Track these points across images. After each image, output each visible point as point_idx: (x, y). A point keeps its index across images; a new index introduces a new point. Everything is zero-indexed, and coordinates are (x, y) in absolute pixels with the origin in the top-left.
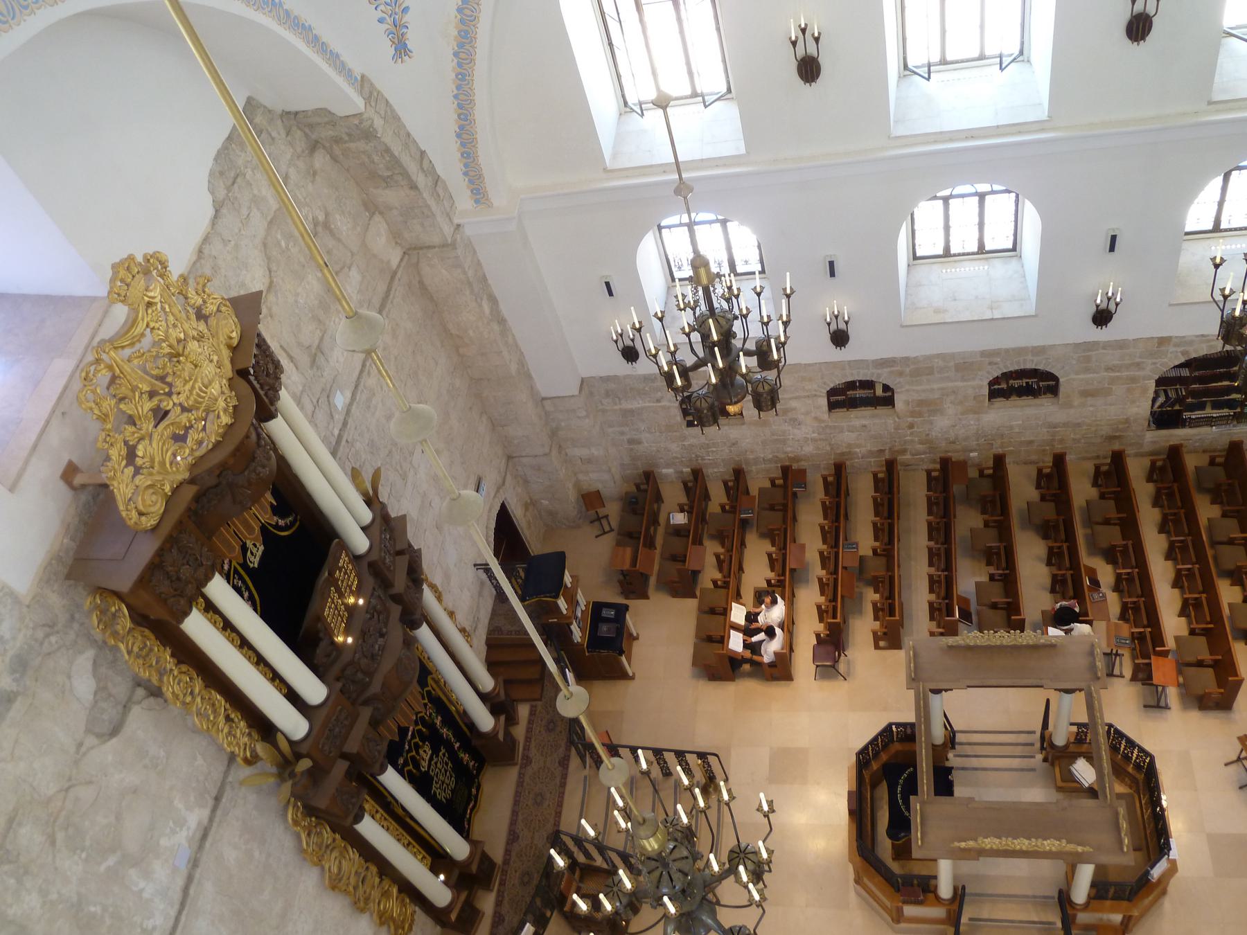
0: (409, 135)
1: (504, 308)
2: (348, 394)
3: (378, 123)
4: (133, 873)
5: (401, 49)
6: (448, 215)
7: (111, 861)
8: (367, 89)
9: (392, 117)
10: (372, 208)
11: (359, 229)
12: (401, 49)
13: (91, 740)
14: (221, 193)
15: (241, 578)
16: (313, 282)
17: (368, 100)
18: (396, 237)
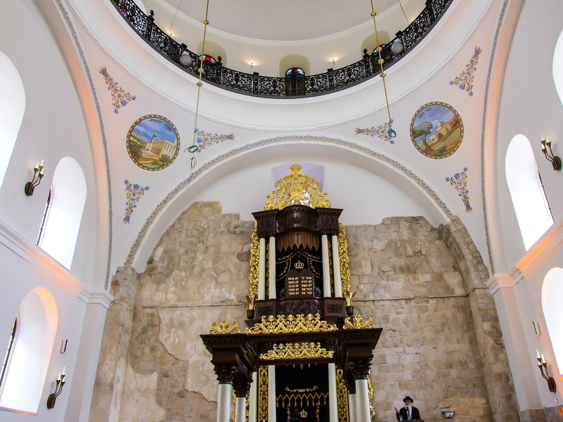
0: (472, 242)
1: (505, 339)
2: (388, 296)
3: (453, 229)
4: (214, 283)
5: (468, 207)
6: (481, 279)
7: (214, 275)
8: (454, 218)
9: (464, 232)
10: (456, 268)
11: (443, 269)
12: (468, 207)
13: (236, 255)
14: (388, 222)
15: (289, 263)
16: (402, 262)
17: (453, 221)
18: (464, 284)
